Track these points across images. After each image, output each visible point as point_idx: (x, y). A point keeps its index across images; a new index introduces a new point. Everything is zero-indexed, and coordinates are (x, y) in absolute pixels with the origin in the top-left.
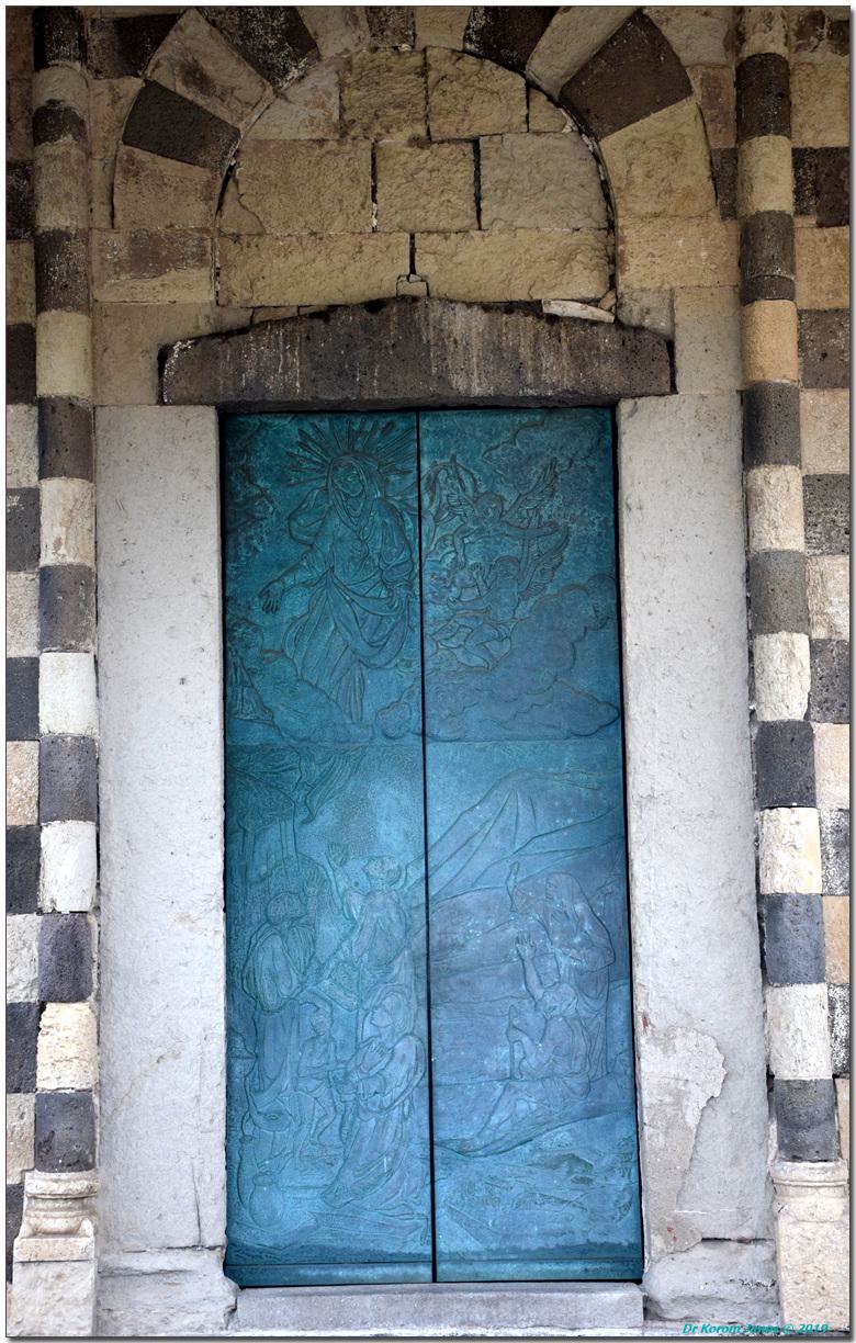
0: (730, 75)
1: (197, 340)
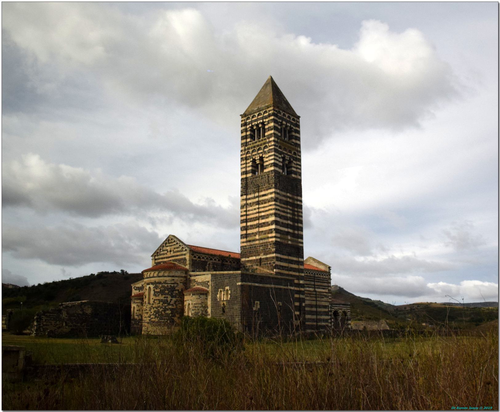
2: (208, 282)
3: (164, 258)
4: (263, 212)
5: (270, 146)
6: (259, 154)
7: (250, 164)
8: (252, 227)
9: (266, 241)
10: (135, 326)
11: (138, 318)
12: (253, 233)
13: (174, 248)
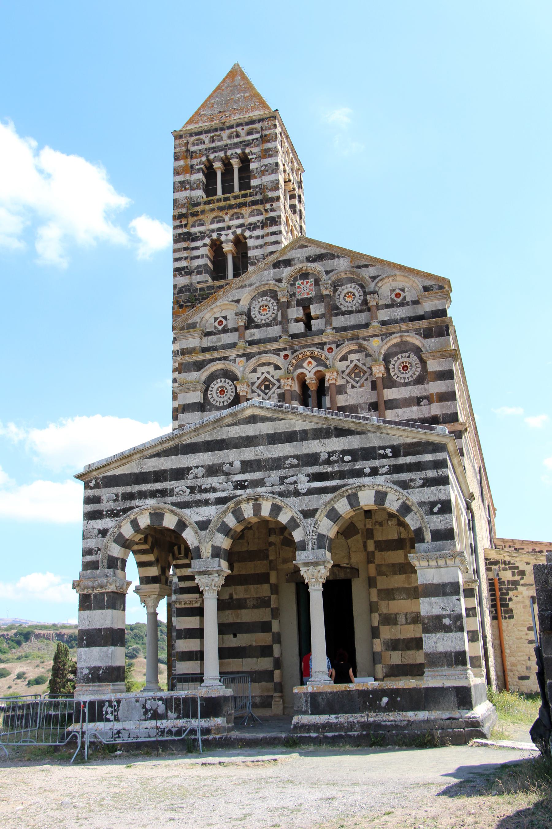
0: (365, 530)
1: (292, 573)
7: (205, 251)
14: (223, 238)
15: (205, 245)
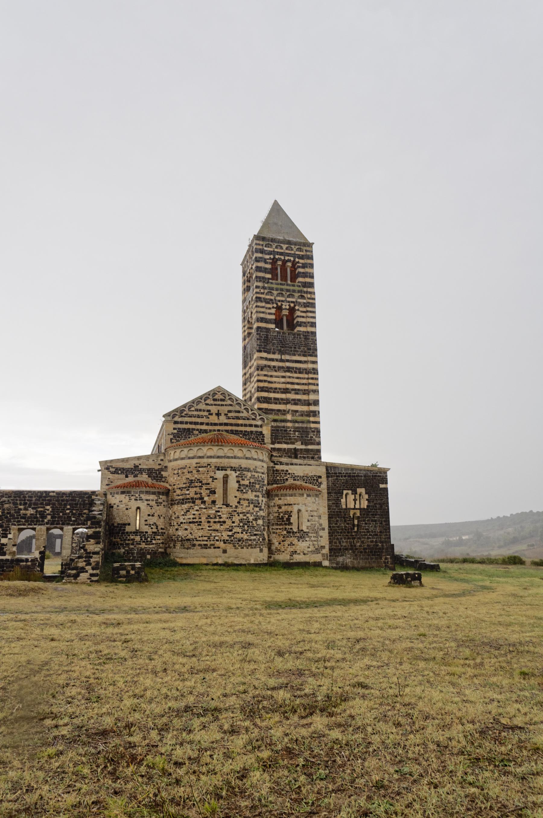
2: (320, 477)
3: (202, 424)
4: (298, 384)
5: (309, 299)
6: (289, 302)
7: (273, 311)
8: (277, 401)
9: (305, 425)
10: (143, 545)
11: (150, 531)
12: (279, 410)
13: (230, 411)
14: (284, 307)
15: (273, 307)
